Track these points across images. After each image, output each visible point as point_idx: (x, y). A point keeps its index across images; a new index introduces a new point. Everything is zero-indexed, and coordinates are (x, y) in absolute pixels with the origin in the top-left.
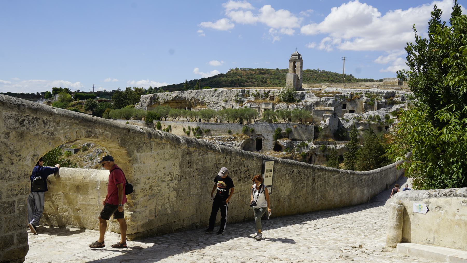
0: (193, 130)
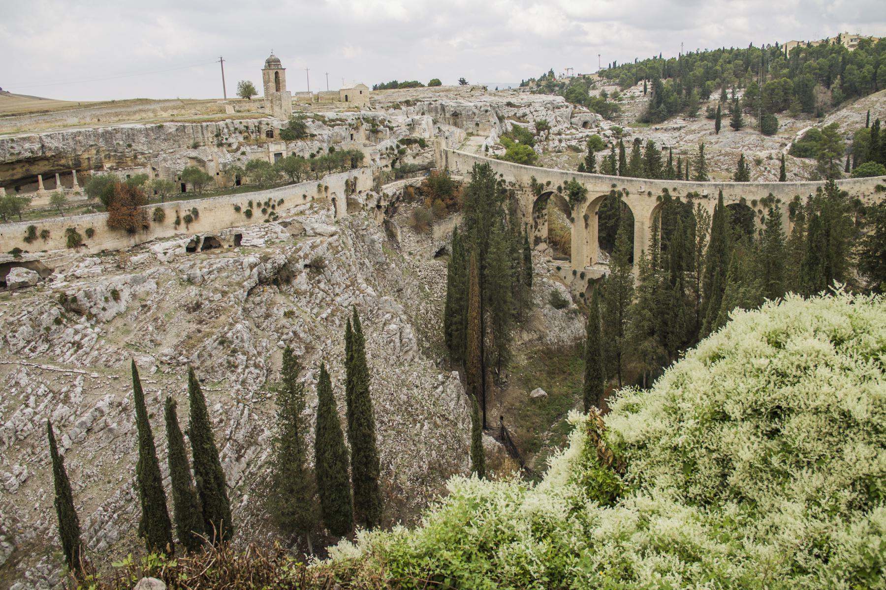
0: (259, 205)
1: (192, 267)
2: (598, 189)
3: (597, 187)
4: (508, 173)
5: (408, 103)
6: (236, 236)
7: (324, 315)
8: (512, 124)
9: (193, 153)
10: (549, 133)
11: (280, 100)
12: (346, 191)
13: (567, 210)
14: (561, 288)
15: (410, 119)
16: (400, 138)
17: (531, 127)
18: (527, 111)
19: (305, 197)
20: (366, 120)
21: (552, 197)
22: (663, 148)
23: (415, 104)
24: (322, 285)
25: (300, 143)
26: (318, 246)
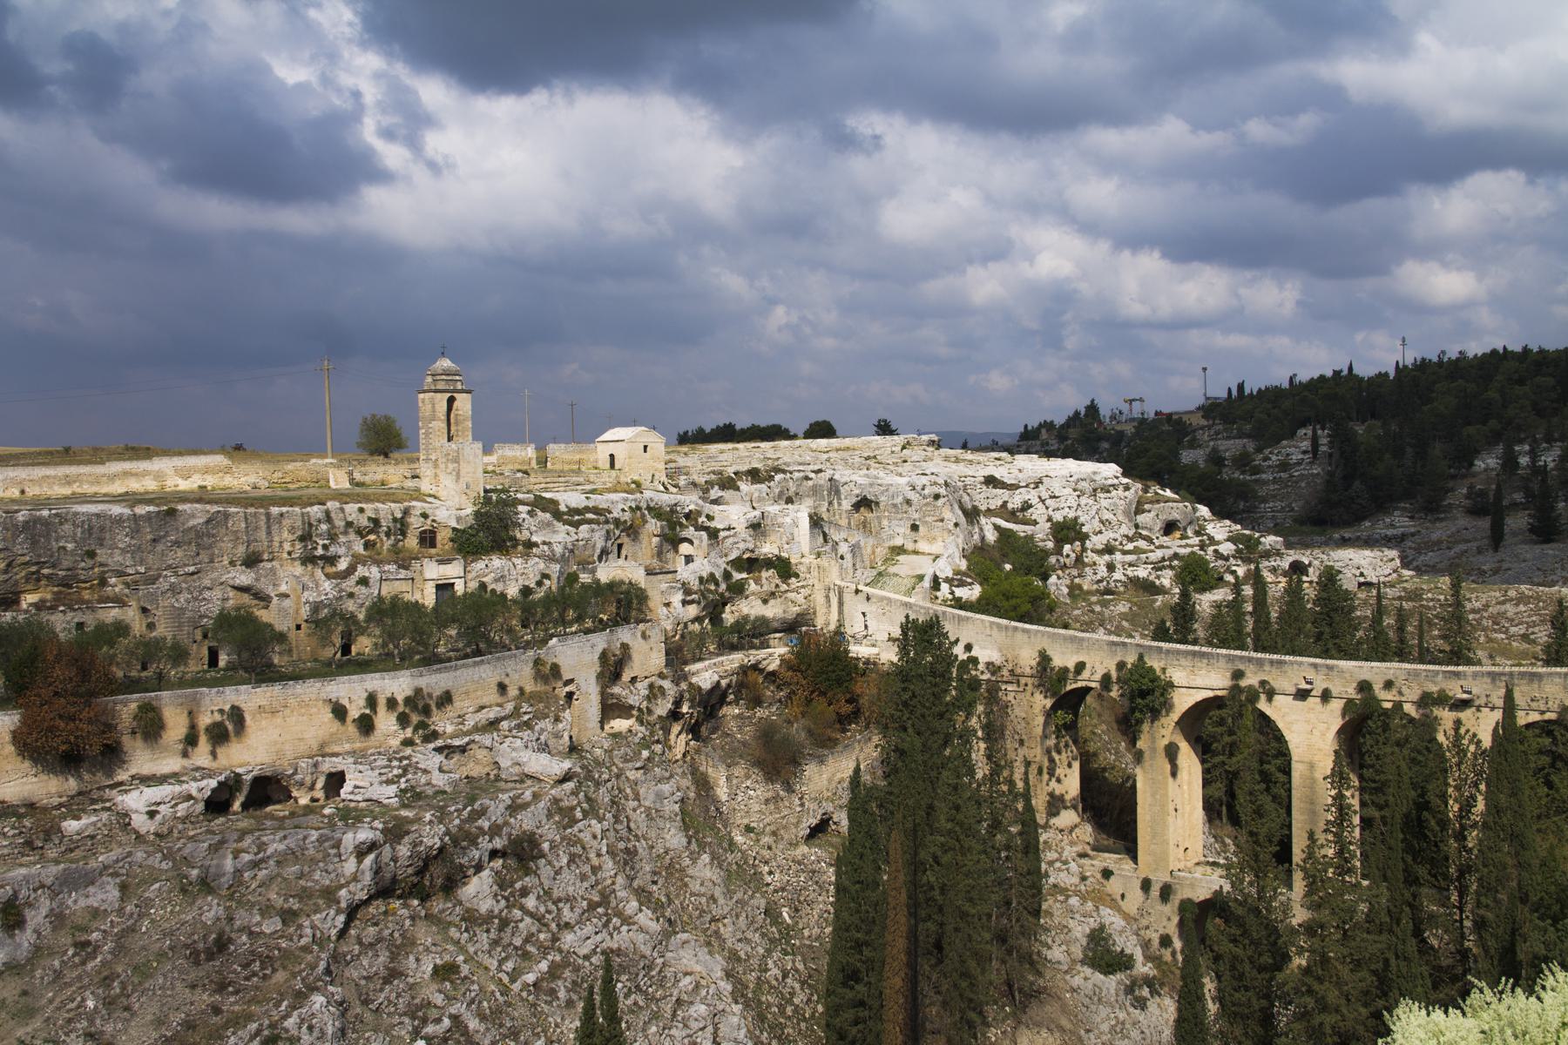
0: (391, 703)
1: (215, 848)
2: (1199, 682)
3: (1196, 679)
4: (984, 641)
5: (754, 475)
6: (331, 776)
7: (530, 978)
8: (997, 527)
9: (244, 578)
10: (1084, 550)
11: (456, 460)
12: (600, 676)
13: (1129, 726)
14: (1110, 918)
15: (757, 513)
16: (733, 556)
17: (1041, 533)
18: (1032, 496)
19: (502, 688)
20: (656, 512)
21: (1089, 699)
22: (1360, 585)
23: (771, 478)
24: (531, 902)
25: (497, 562)
26: (525, 806)
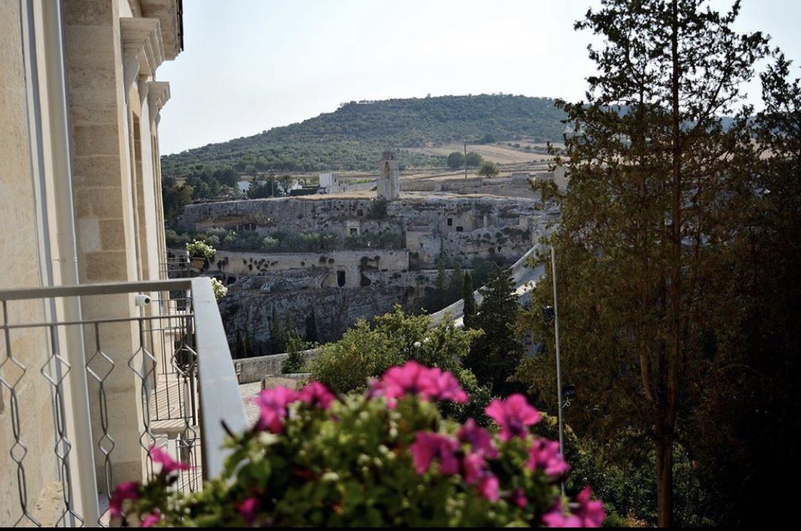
0: (256, 262)
